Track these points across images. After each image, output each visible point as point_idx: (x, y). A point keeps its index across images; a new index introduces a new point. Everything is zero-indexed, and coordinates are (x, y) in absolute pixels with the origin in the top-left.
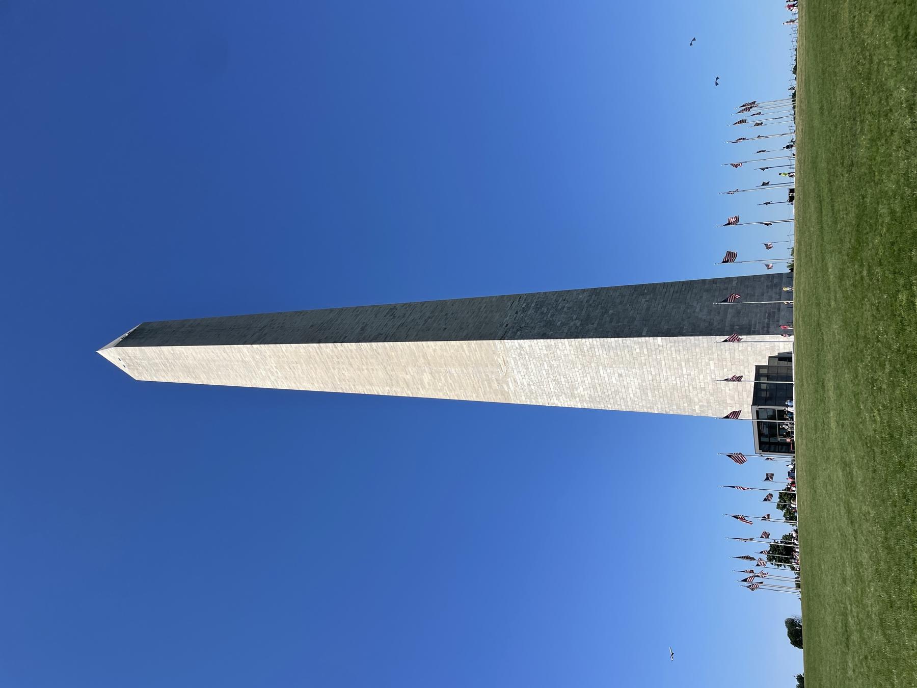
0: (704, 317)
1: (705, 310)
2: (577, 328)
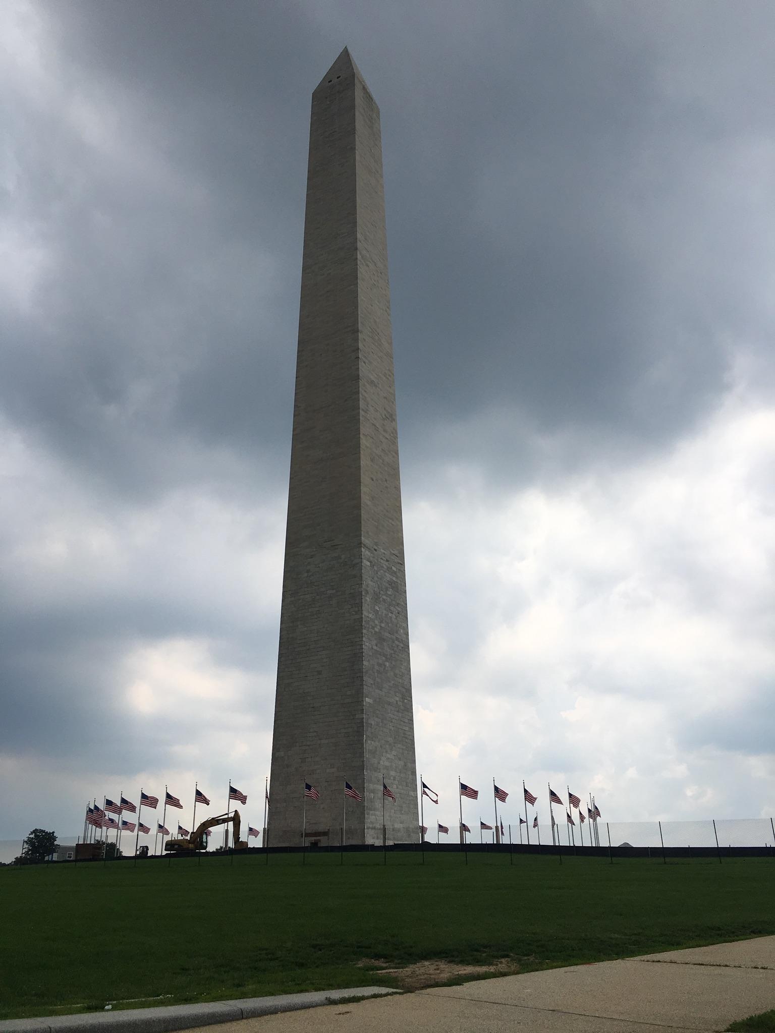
0: (381, 762)
1: (387, 764)
2: (373, 628)
